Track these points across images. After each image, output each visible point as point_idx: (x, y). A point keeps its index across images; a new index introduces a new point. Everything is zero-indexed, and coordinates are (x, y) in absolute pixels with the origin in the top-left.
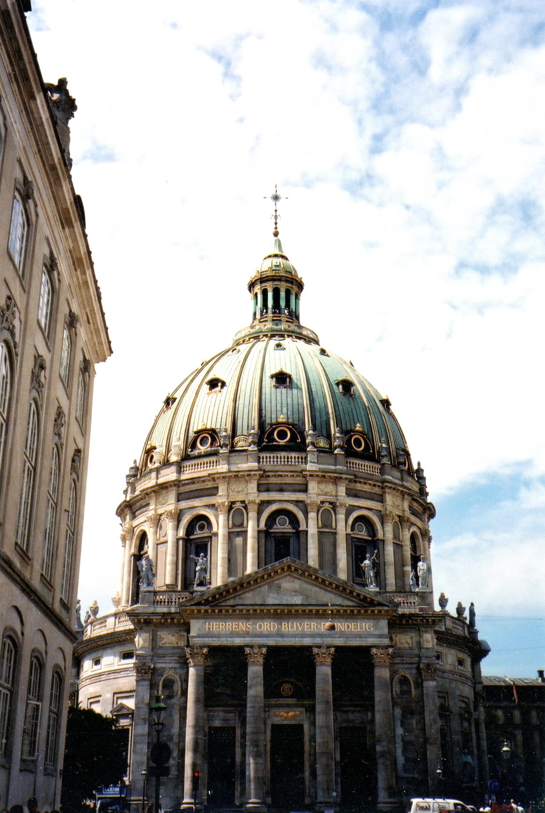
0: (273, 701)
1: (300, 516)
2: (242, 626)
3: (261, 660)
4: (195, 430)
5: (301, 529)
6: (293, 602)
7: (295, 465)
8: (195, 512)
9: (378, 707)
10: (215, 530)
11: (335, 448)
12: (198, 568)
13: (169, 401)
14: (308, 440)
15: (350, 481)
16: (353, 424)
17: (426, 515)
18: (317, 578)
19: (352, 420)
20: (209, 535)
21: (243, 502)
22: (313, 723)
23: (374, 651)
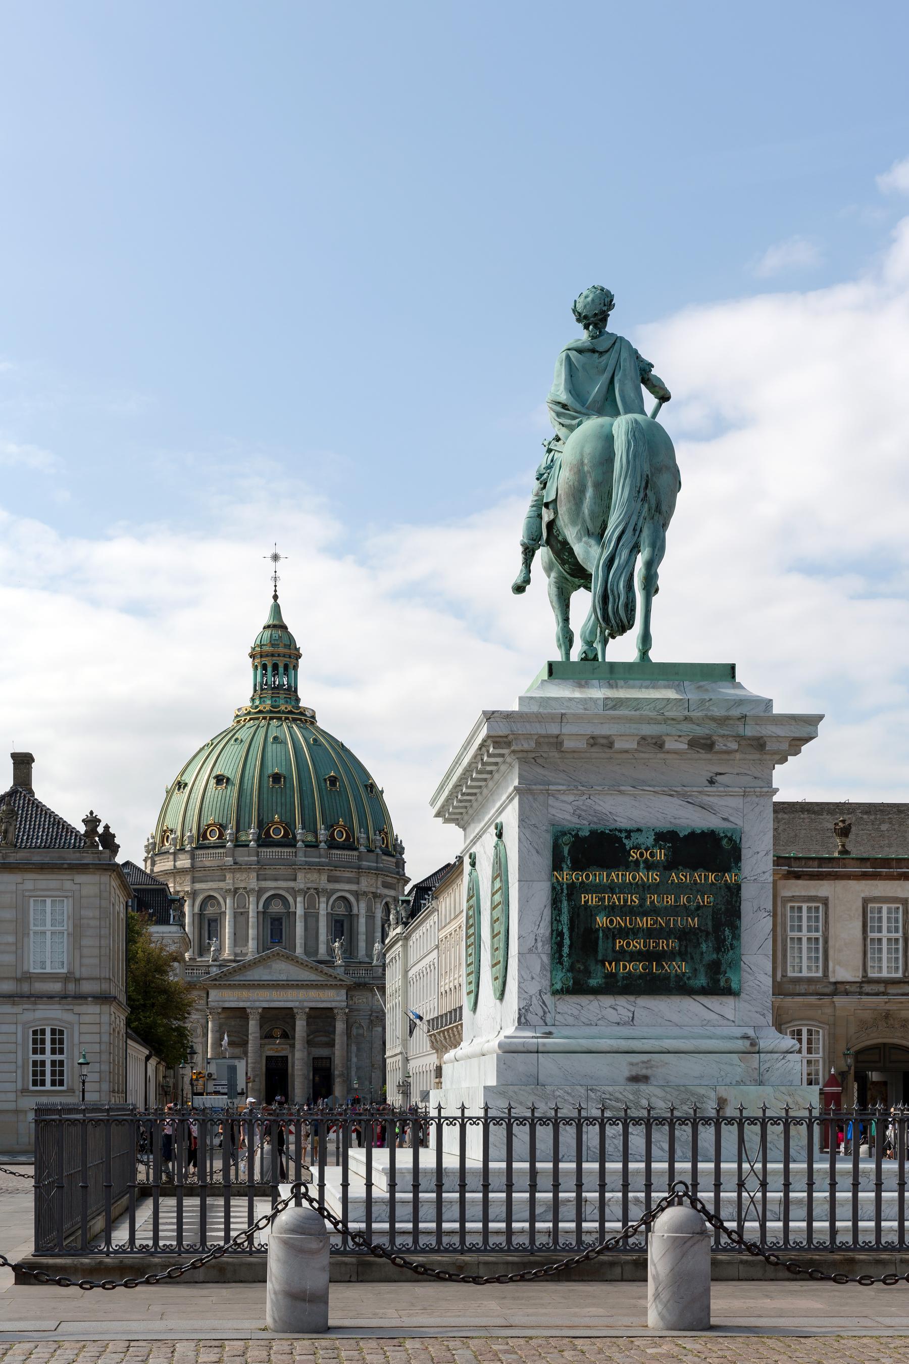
0: (267, 1041)
1: (291, 899)
2: (245, 994)
3: (258, 1017)
4: (205, 824)
5: (290, 910)
6: (281, 979)
7: (287, 859)
8: (207, 894)
9: (337, 1047)
10: (223, 909)
11: (321, 842)
12: (212, 949)
13: (180, 785)
14: (298, 837)
15: (332, 870)
16: (336, 818)
17: (400, 884)
18: (297, 962)
19: (336, 814)
20: (219, 912)
21: (245, 888)
22: (293, 1055)
23: (336, 1011)
